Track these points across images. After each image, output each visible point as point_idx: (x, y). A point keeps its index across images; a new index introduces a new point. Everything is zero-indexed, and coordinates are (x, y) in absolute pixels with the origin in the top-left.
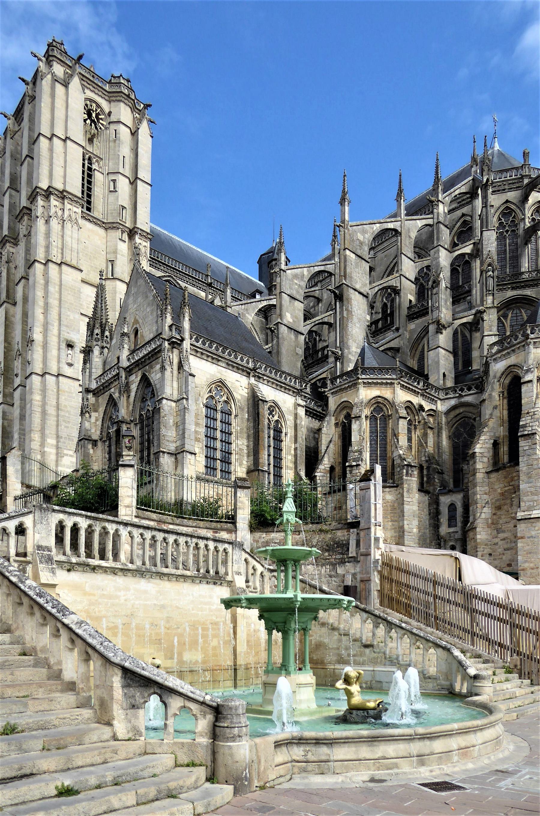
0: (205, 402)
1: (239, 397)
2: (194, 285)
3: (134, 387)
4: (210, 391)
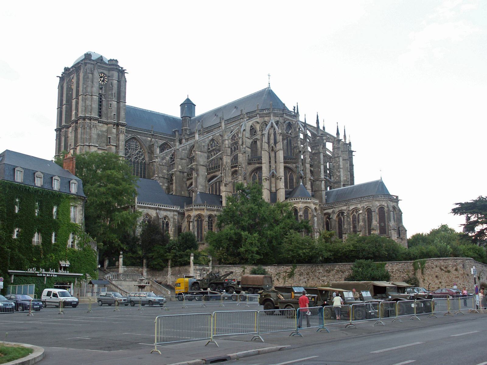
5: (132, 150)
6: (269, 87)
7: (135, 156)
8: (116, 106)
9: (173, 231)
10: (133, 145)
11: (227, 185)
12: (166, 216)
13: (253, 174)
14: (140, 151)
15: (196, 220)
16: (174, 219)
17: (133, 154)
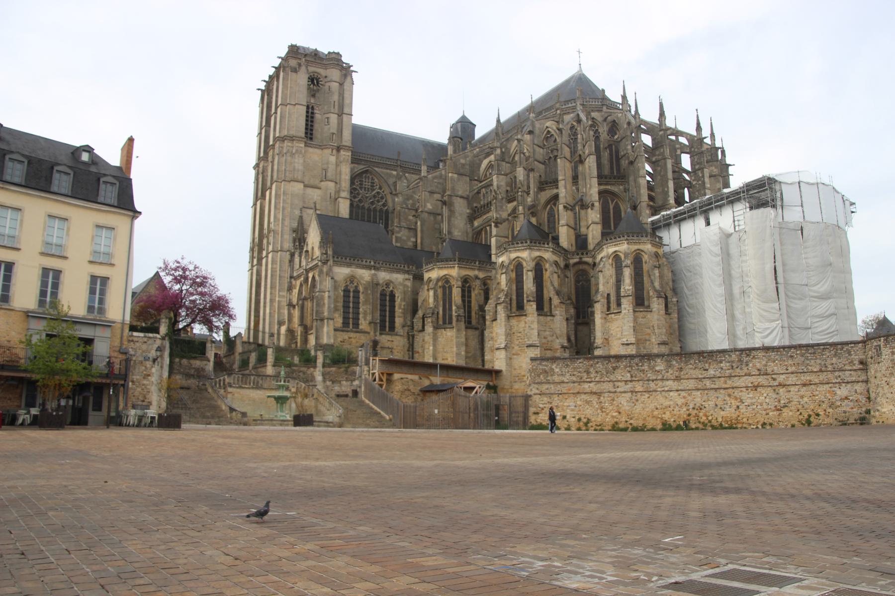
0: (343, 289)
1: (365, 282)
2: (387, 169)
3: (310, 280)
4: (346, 282)
5: (365, 190)
6: (581, 70)
7: (370, 199)
8: (336, 121)
9: (402, 307)
10: (367, 183)
11: (499, 225)
12: (388, 280)
13: (549, 206)
14: (378, 193)
15: (440, 287)
16: (405, 286)
17: (367, 197)
